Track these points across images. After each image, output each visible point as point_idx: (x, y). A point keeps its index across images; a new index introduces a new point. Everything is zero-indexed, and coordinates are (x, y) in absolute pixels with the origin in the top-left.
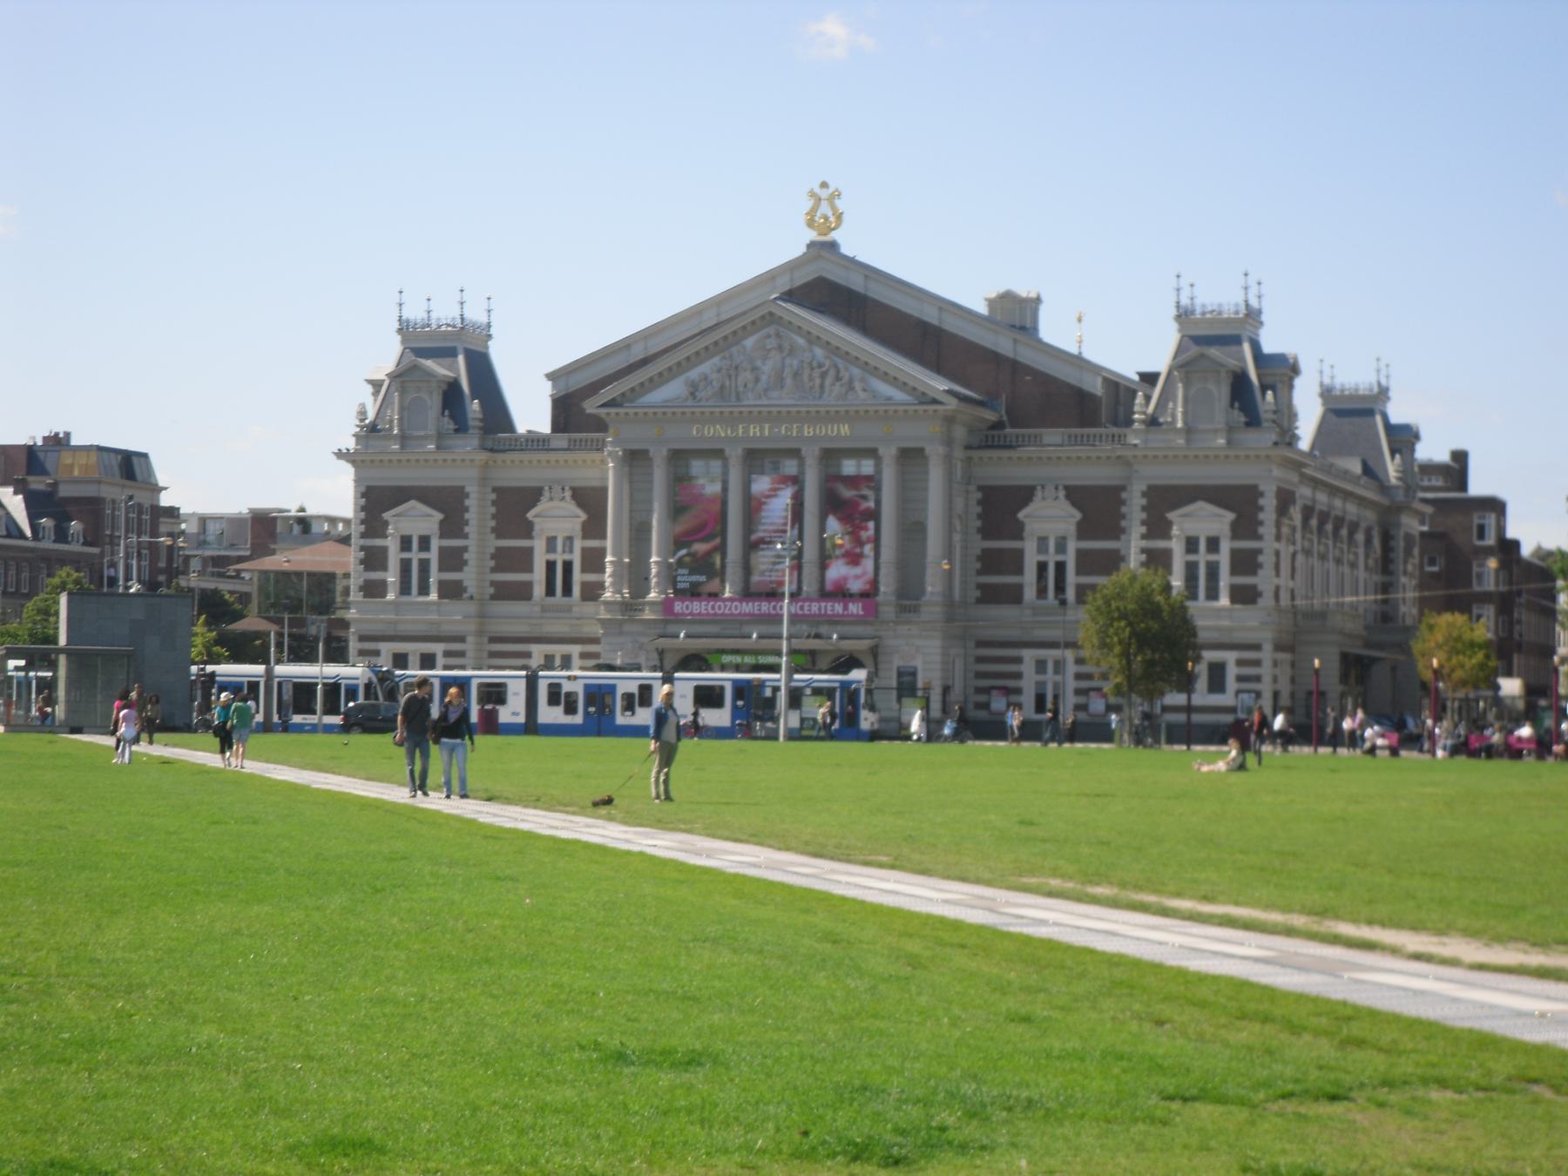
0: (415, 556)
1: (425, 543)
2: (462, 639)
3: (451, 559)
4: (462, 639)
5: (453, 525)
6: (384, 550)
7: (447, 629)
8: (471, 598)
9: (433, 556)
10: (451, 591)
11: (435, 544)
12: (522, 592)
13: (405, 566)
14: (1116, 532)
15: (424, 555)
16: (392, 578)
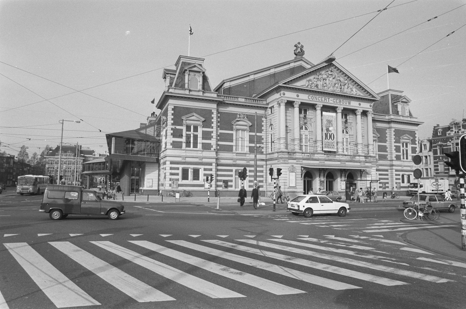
0: (192, 132)
1: (196, 129)
2: (210, 164)
3: (207, 136)
4: (210, 164)
5: (207, 123)
6: (182, 130)
7: (205, 160)
8: (215, 150)
9: (200, 134)
10: (206, 147)
11: (200, 130)
12: (229, 149)
13: (188, 137)
14: (385, 141)
15: (196, 133)
16: (184, 139)
